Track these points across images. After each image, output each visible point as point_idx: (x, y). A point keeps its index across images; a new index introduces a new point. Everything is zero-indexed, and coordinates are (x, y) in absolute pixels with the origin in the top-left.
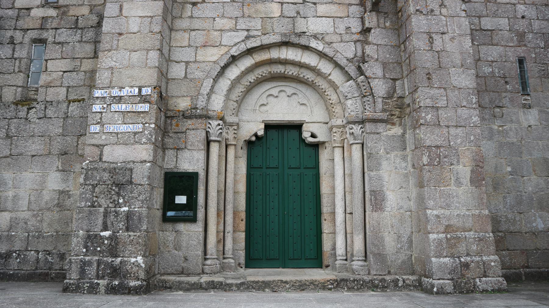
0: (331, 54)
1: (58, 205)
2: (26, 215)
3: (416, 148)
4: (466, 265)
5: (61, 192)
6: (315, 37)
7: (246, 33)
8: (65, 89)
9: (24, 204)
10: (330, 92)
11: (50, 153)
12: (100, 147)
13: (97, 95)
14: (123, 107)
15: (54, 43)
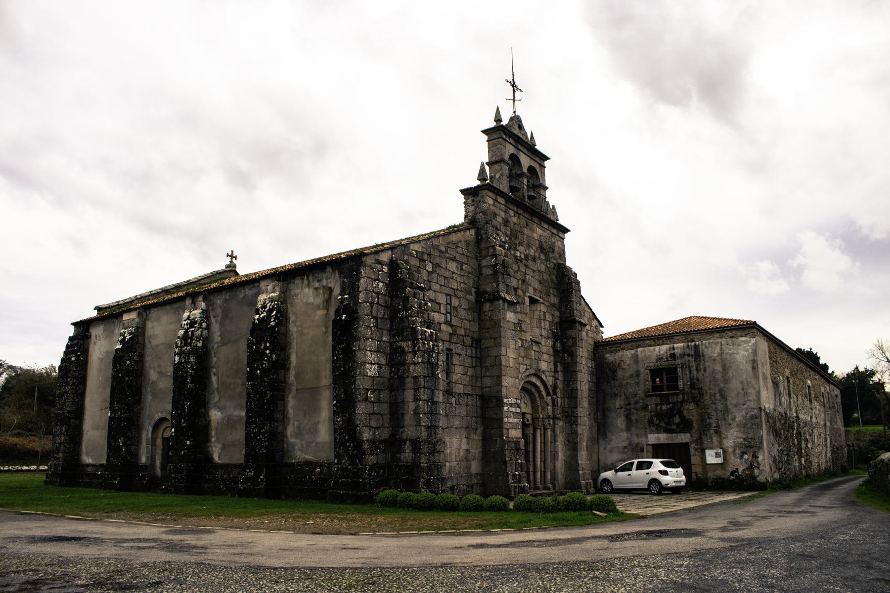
0: (547, 382)
1: (466, 458)
2: (454, 464)
3: (572, 433)
4: (587, 483)
5: (467, 451)
6: (543, 372)
7: (525, 367)
8: (462, 386)
9: (453, 457)
10: (538, 399)
11: (462, 427)
12: (507, 429)
13: (505, 402)
14: (512, 409)
15: (456, 353)
